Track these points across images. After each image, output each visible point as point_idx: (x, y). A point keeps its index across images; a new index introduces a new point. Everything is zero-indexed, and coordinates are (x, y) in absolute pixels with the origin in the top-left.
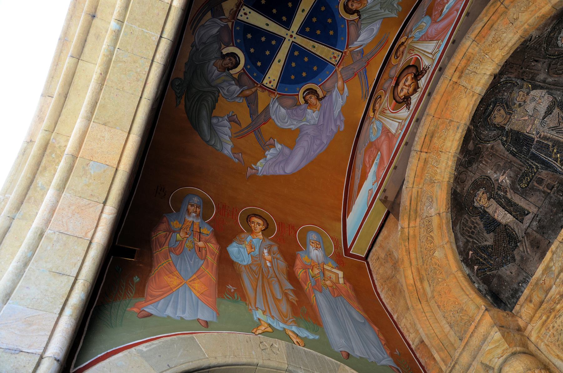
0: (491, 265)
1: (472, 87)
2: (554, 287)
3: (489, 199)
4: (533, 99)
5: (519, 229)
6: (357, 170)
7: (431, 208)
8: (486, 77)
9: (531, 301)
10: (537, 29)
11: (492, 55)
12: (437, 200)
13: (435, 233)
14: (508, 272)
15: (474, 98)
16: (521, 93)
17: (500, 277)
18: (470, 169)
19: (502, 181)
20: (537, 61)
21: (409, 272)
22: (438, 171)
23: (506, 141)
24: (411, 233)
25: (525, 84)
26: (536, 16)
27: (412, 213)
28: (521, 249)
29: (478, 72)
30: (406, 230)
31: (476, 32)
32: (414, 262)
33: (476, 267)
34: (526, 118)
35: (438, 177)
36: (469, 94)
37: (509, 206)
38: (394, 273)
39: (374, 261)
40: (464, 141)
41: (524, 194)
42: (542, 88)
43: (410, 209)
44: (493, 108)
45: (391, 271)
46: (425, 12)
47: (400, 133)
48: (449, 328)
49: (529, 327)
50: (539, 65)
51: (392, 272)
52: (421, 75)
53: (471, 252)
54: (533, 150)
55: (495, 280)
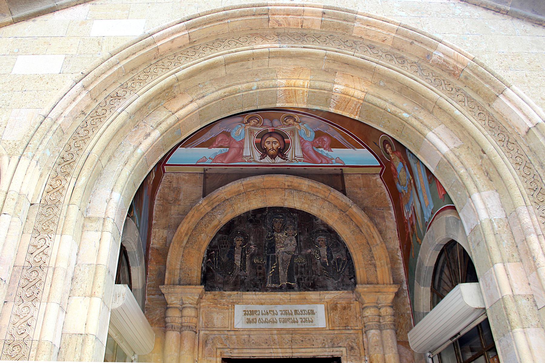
0: (216, 268)
1: (286, 200)
2: (225, 300)
3: (241, 246)
4: (291, 240)
5: (237, 272)
6: (209, 132)
7: (220, 215)
8: (293, 206)
9: (214, 296)
10: (322, 221)
11: (304, 203)
12: (225, 215)
13: (211, 226)
14: (218, 278)
15: (281, 204)
16: (292, 231)
17: (213, 275)
18: (248, 223)
19: (251, 248)
20: (308, 231)
21: (185, 225)
22: (239, 205)
23: (269, 237)
24: (202, 210)
25: (297, 231)
26: (327, 219)
27: (211, 202)
28: (230, 278)
29: (295, 199)
30: (202, 206)
31: (313, 185)
32: (191, 223)
33: (209, 260)
34: (282, 242)
35: (235, 206)
36: (282, 199)
37: (243, 258)
38: (172, 202)
39: (167, 180)
40: (259, 209)
41: (252, 263)
42: (297, 242)
43: (212, 200)
44: (281, 218)
45: (171, 199)
46: (316, 130)
47: (246, 162)
48: (179, 268)
49: (204, 300)
50: (306, 234)
51: (171, 201)
52: (282, 155)
53: (214, 252)
54: (271, 255)
55: (211, 274)
